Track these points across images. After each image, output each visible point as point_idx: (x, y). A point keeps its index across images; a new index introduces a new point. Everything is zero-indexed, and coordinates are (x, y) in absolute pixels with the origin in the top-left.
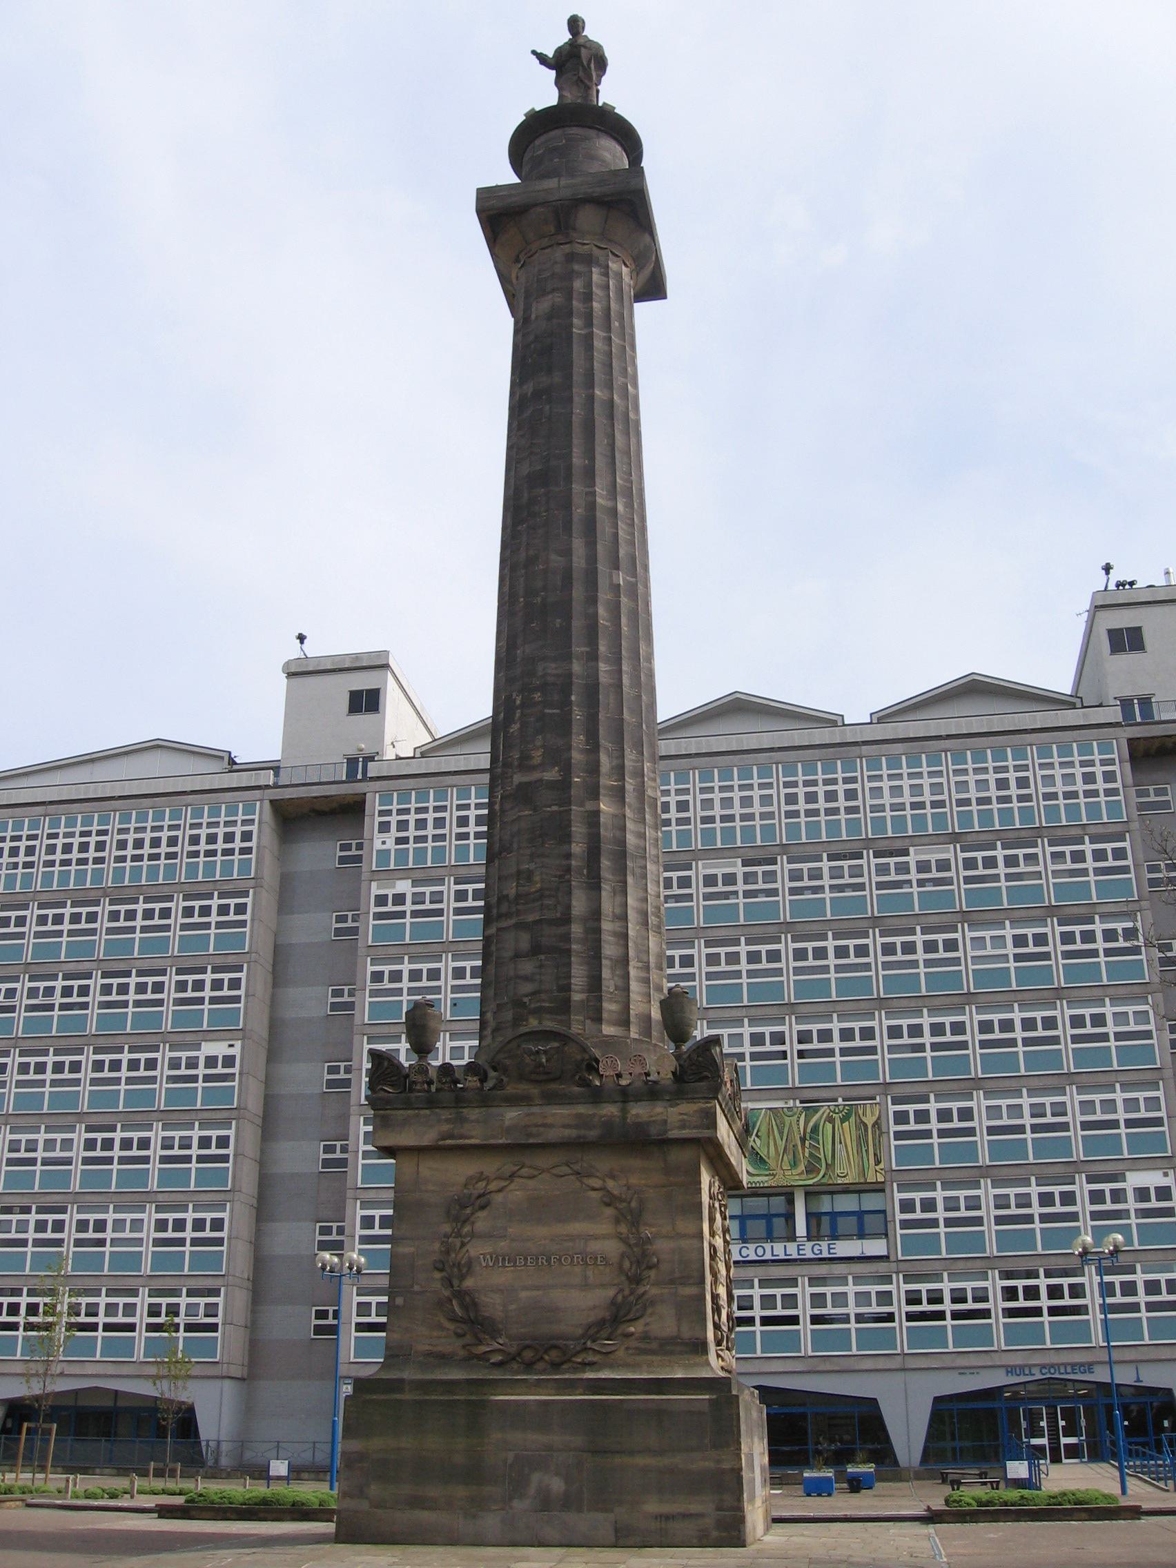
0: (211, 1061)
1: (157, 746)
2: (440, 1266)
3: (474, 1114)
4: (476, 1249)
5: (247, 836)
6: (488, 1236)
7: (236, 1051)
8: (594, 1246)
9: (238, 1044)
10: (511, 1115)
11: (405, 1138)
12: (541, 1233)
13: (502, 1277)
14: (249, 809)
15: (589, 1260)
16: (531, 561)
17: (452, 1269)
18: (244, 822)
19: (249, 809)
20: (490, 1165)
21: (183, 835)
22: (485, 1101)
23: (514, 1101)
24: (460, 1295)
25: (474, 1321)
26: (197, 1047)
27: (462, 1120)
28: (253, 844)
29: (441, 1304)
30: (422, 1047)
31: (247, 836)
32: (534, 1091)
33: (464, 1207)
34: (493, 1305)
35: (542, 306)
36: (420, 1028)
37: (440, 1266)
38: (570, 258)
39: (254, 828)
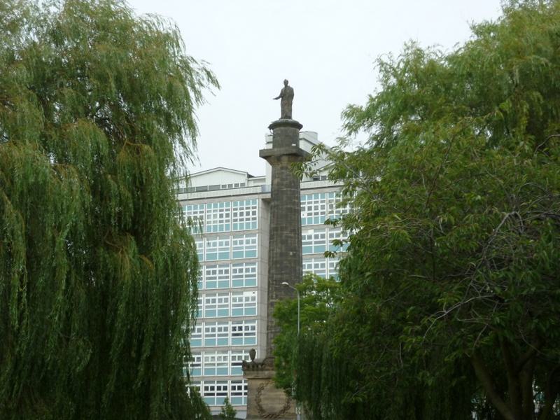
0: (247, 299)
1: (219, 170)
2: (256, 400)
3: (260, 372)
4: (262, 397)
5: (254, 213)
6: (264, 395)
7: (256, 294)
8: (281, 397)
9: (256, 292)
10: (267, 372)
11: (249, 377)
12: (272, 394)
13: (266, 402)
14: (254, 202)
15: (280, 399)
16: (273, 250)
17: (258, 400)
18: (253, 208)
19: (254, 202)
20: (263, 382)
21: (231, 213)
22: (262, 370)
23: (267, 370)
24: (259, 405)
25: (261, 410)
26: (242, 293)
27: (258, 374)
28: (257, 216)
29: (256, 407)
30: (253, 358)
31: (254, 213)
32: (271, 368)
33: (260, 389)
34: (264, 407)
35: (276, 181)
36: (253, 353)
37: (256, 400)
38: (282, 168)
39: (257, 210)
